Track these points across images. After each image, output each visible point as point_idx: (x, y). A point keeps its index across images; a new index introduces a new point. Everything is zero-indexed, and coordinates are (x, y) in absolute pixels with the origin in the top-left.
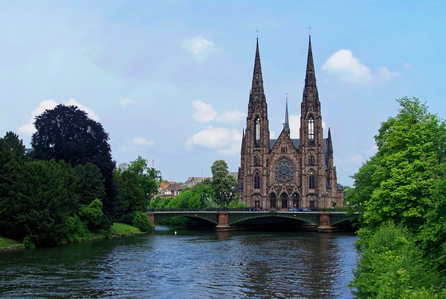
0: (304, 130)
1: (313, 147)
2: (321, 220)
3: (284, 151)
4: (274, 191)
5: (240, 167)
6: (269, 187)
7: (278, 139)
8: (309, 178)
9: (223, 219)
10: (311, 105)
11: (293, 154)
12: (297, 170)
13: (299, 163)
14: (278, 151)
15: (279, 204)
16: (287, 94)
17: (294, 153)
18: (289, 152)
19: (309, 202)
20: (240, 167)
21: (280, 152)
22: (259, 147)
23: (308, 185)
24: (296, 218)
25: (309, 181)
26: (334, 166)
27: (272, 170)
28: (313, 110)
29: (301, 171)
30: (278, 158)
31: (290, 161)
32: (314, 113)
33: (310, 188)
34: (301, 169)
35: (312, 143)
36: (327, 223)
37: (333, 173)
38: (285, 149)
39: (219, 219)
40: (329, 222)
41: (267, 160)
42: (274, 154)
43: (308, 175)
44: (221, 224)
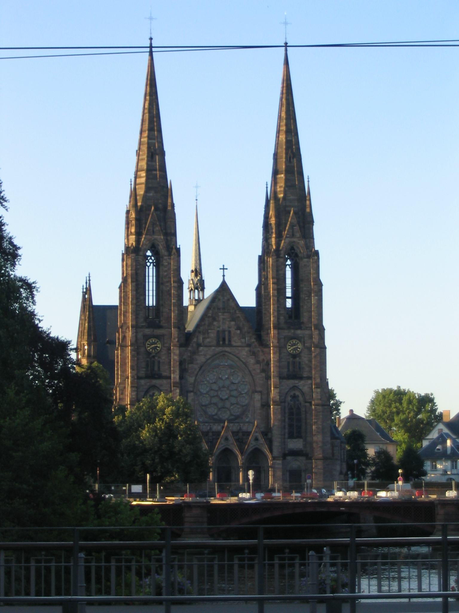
1: (299, 332)
3: (224, 340)
8: (287, 411)
11: (247, 349)
12: (259, 389)
13: (263, 371)
14: (208, 340)
16: (197, 187)
17: (249, 345)
18: (236, 341)
19: (288, 474)
21: (214, 342)
22: (160, 327)
23: (287, 431)
25: (289, 419)
27: (191, 389)
28: (298, 235)
30: (208, 357)
33: (291, 436)
38: (227, 333)
41: (181, 363)
42: (199, 345)
43: (286, 404)
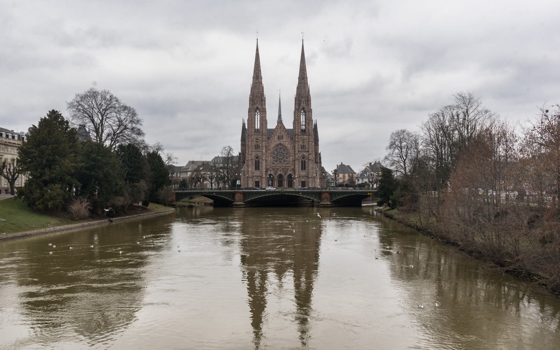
0: (296, 121)
2: (322, 197)
4: (272, 173)
5: (240, 152)
6: (267, 170)
7: (275, 128)
9: (239, 197)
10: (303, 100)
15: (285, 183)
20: (240, 152)
24: (302, 196)
26: (319, 152)
29: (295, 156)
31: (285, 148)
32: (305, 107)
34: (295, 155)
35: (303, 131)
36: (328, 199)
37: (318, 158)
39: (235, 197)
40: (329, 198)
44: (237, 201)
